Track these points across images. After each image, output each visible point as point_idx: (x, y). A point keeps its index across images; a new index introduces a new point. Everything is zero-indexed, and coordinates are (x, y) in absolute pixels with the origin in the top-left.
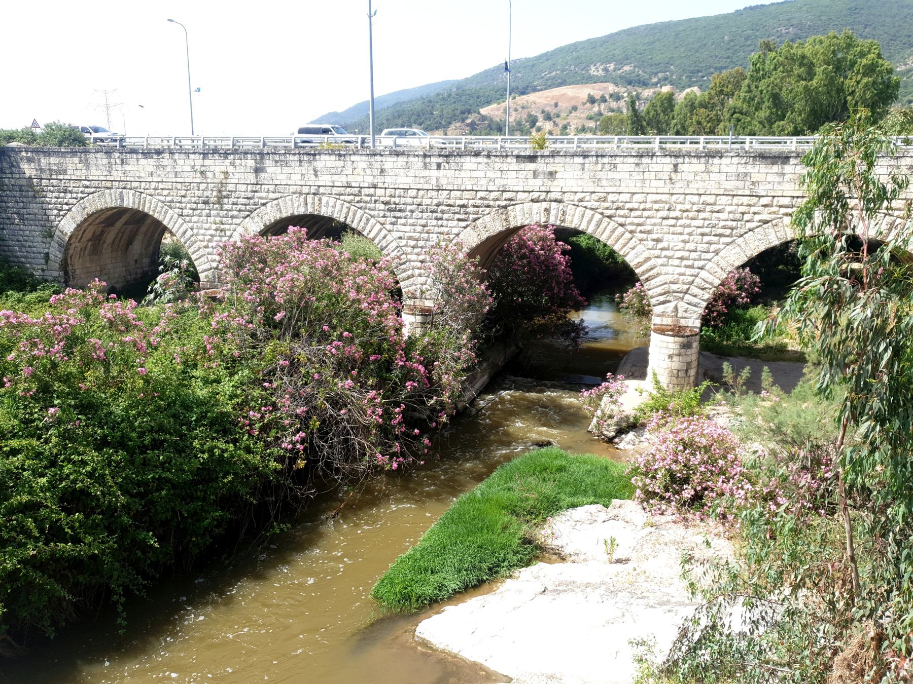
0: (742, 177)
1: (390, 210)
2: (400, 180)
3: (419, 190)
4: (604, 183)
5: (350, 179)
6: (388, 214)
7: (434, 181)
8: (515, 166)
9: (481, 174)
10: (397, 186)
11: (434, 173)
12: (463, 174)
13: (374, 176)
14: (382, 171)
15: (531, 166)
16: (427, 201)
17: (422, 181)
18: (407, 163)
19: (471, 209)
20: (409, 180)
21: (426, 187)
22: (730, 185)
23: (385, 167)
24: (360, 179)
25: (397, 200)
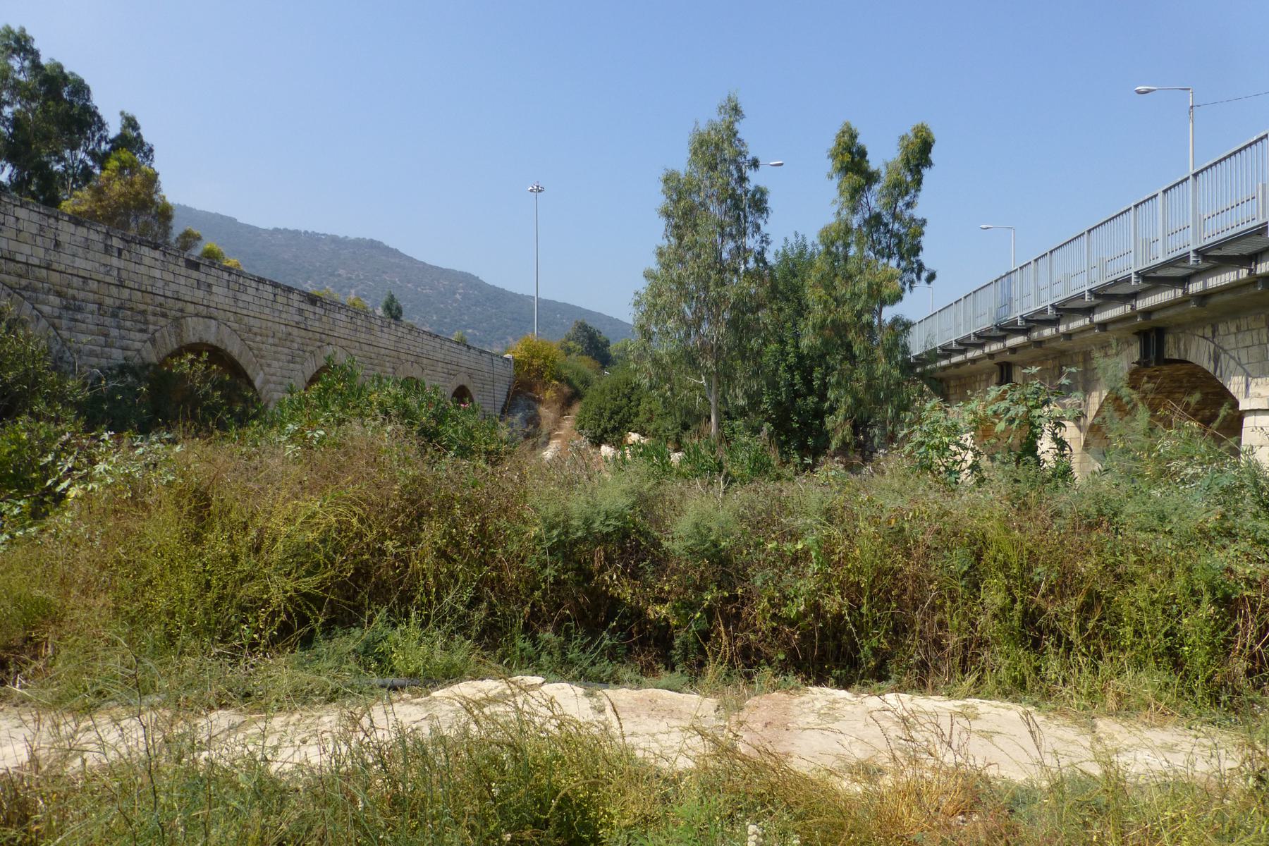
0: (301, 311)
1: (67, 308)
2: (79, 263)
3: (99, 281)
4: (240, 304)
5: (13, 246)
6: (64, 313)
7: (115, 273)
8: (184, 271)
9: (157, 274)
10: (75, 272)
11: (115, 261)
12: (143, 269)
13: (47, 250)
14: (57, 244)
15: (194, 274)
16: (109, 301)
17: (102, 269)
18: (87, 239)
19: (151, 318)
20: (89, 265)
21: (108, 279)
22: (297, 318)
23: (60, 239)
24: (26, 249)
25: (75, 292)
